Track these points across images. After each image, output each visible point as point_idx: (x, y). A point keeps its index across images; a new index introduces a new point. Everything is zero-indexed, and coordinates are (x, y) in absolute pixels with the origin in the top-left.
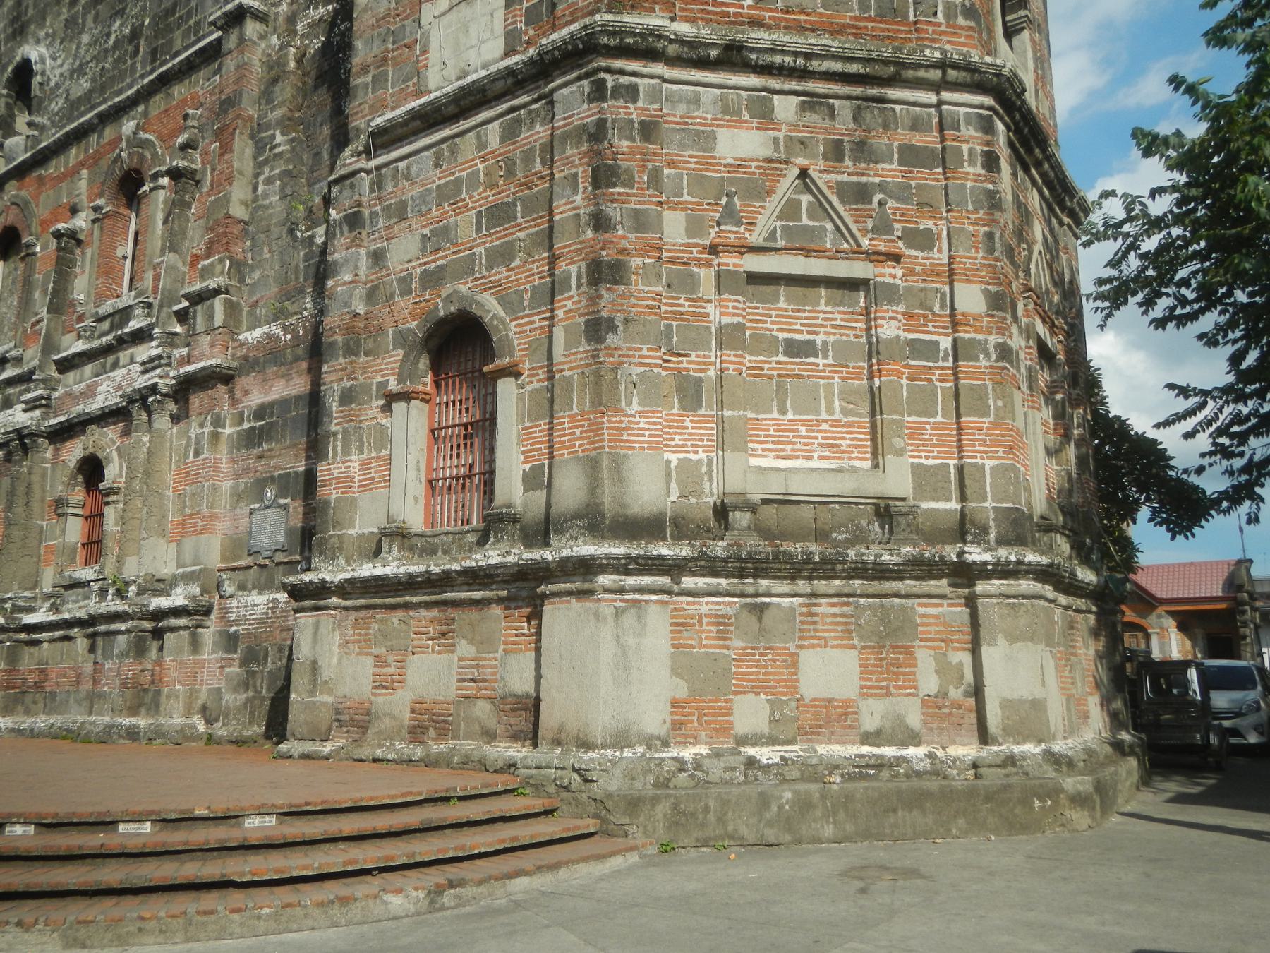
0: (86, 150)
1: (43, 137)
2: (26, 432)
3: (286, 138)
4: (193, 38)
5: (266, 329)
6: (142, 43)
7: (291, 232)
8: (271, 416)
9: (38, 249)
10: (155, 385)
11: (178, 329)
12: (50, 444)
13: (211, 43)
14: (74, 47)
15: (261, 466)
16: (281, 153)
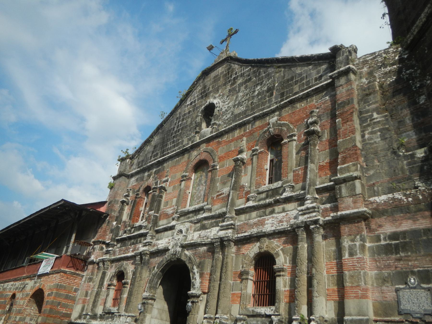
0: (244, 131)
1: (220, 128)
2: (226, 239)
3: (381, 115)
4: (305, 87)
5: (390, 196)
6: (275, 91)
7: (394, 153)
8: (405, 238)
9: (218, 167)
10: (319, 219)
11: (317, 196)
12: (235, 245)
13: (322, 85)
14: (235, 97)
15: (400, 265)
16: (379, 122)
